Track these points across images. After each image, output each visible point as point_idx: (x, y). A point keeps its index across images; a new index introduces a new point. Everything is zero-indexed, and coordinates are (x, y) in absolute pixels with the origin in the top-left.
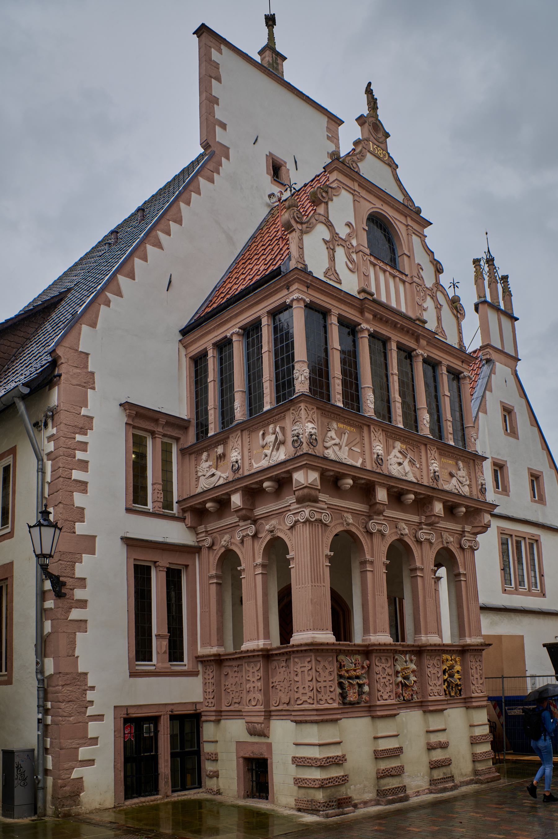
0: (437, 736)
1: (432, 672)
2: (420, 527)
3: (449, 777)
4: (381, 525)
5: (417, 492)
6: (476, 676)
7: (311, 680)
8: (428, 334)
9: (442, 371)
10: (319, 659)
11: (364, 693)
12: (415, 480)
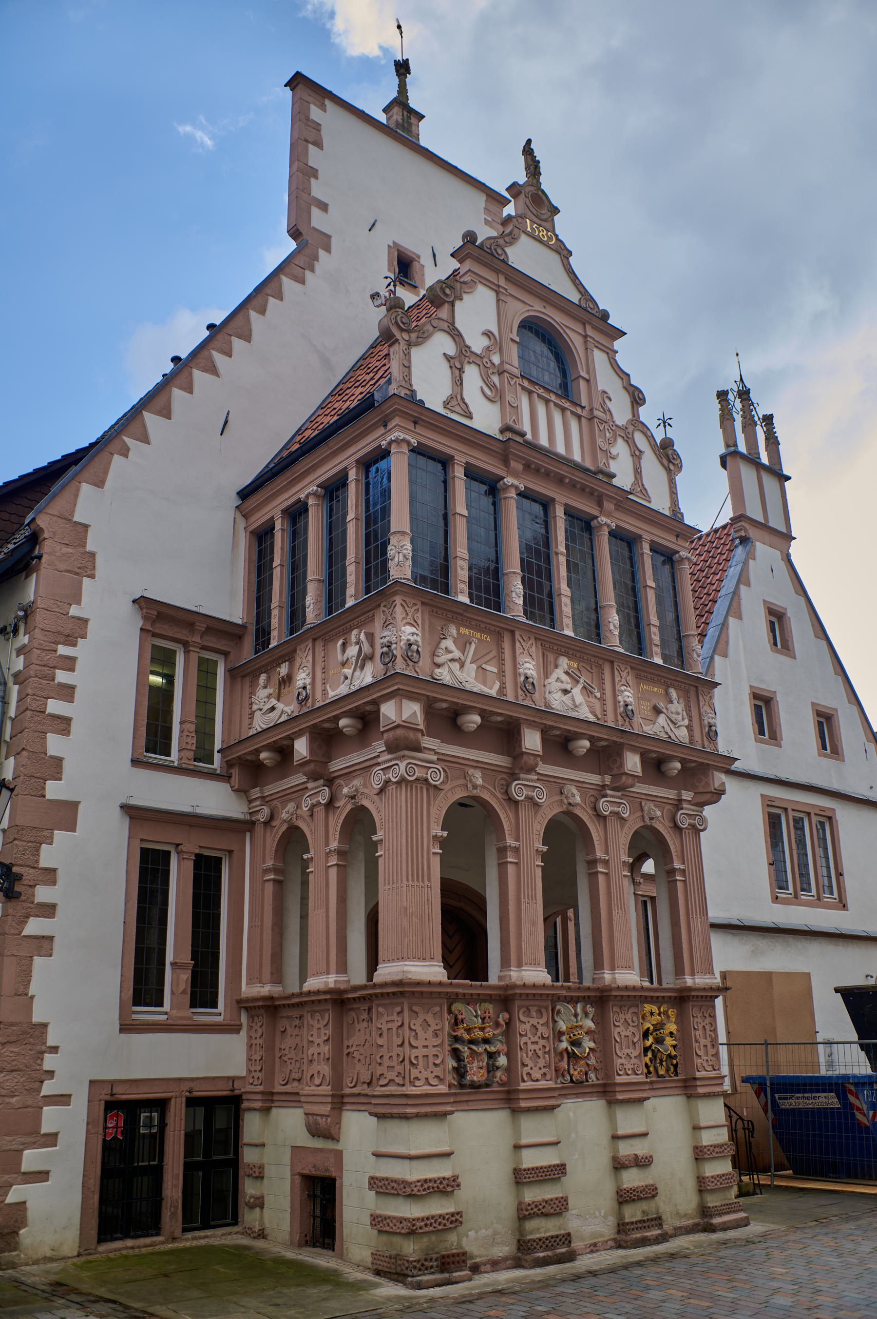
0: (632, 1146)
2: (603, 792)
3: (652, 1220)
4: (532, 789)
5: (593, 736)
6: (703, 1042)
7: (402, 1045)
8: (616, 494)
9: (642, 549)
10: (415, 1008)
11: (498, 1068)
12: (592, 718)
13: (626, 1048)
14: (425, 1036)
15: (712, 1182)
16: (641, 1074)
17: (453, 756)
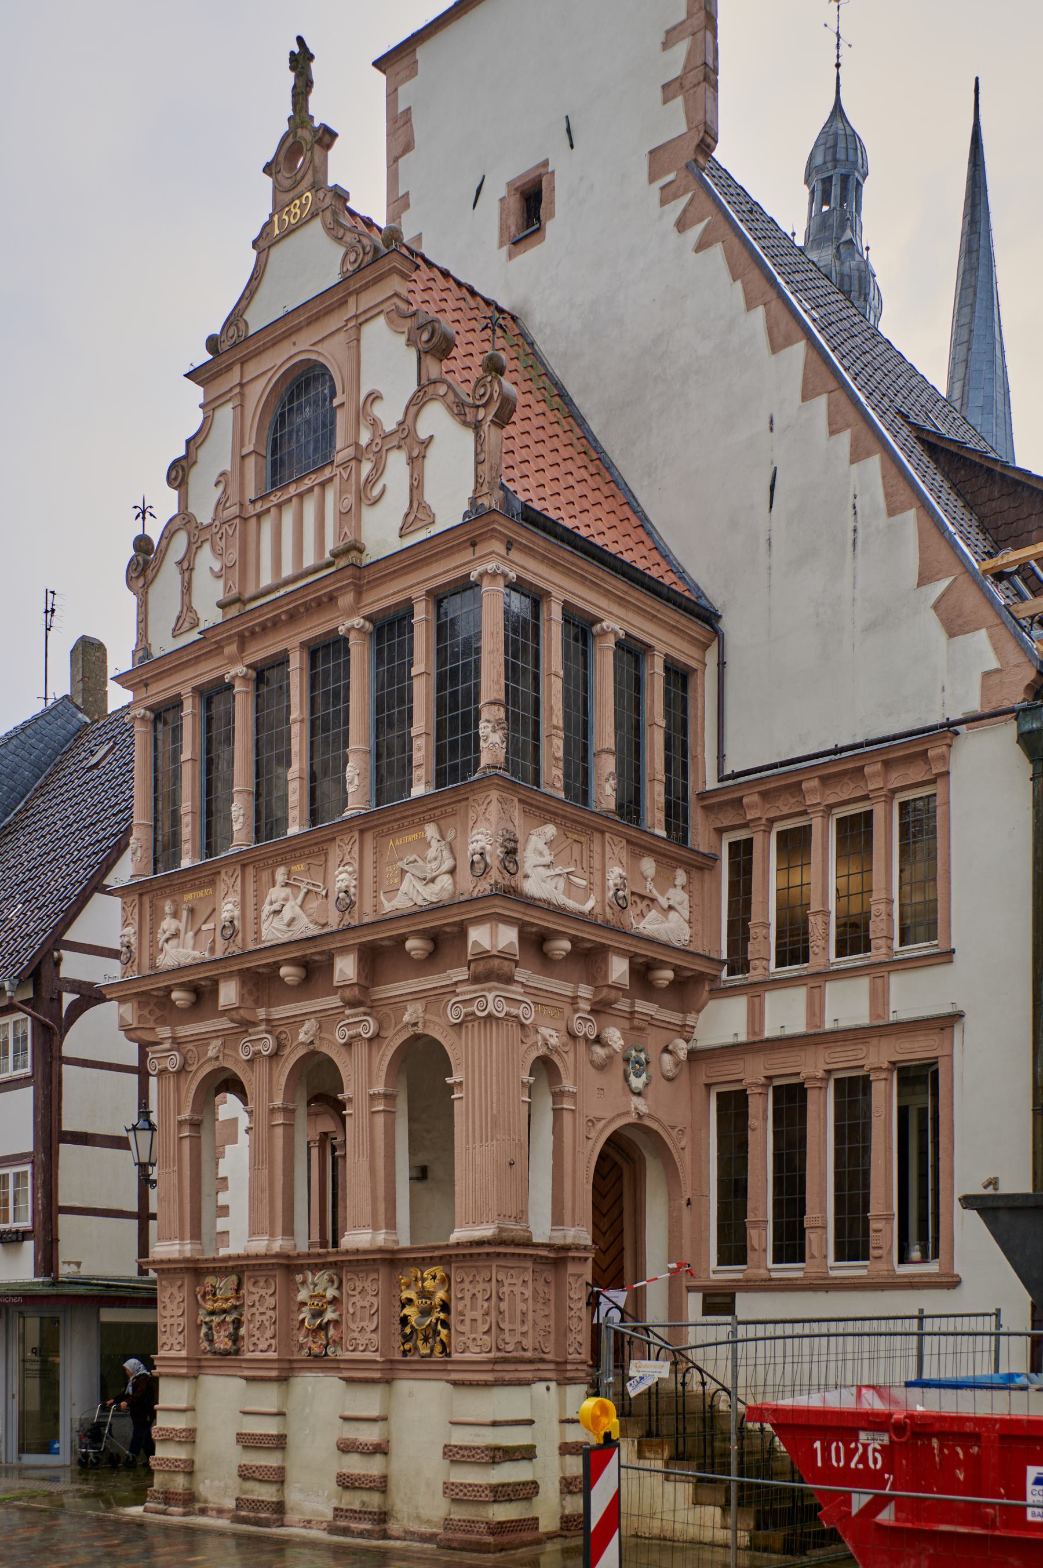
0: (358, 1430)
1: (359, 1304)
3: (370, 1513)
6: (469, 1315)
13: (361, 1320)
14: (172, 1307)
15: (452, 1490)
16: (376, 1351)
17: (193, 1035)
